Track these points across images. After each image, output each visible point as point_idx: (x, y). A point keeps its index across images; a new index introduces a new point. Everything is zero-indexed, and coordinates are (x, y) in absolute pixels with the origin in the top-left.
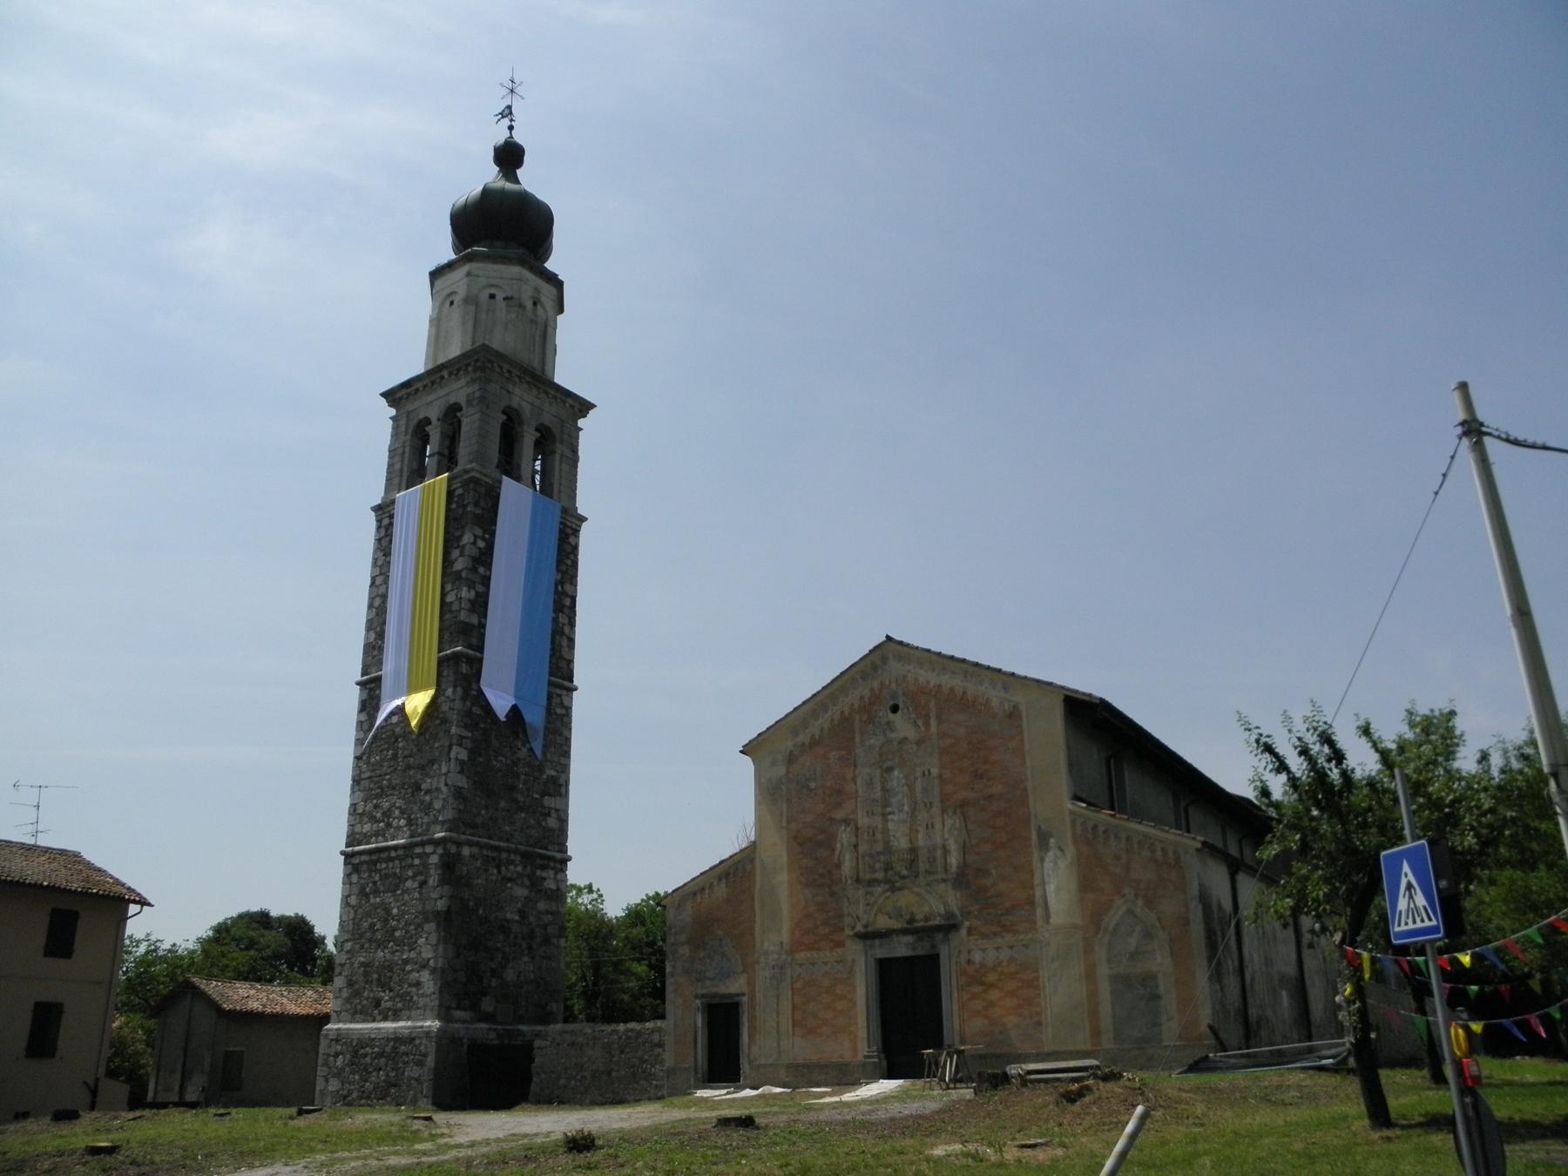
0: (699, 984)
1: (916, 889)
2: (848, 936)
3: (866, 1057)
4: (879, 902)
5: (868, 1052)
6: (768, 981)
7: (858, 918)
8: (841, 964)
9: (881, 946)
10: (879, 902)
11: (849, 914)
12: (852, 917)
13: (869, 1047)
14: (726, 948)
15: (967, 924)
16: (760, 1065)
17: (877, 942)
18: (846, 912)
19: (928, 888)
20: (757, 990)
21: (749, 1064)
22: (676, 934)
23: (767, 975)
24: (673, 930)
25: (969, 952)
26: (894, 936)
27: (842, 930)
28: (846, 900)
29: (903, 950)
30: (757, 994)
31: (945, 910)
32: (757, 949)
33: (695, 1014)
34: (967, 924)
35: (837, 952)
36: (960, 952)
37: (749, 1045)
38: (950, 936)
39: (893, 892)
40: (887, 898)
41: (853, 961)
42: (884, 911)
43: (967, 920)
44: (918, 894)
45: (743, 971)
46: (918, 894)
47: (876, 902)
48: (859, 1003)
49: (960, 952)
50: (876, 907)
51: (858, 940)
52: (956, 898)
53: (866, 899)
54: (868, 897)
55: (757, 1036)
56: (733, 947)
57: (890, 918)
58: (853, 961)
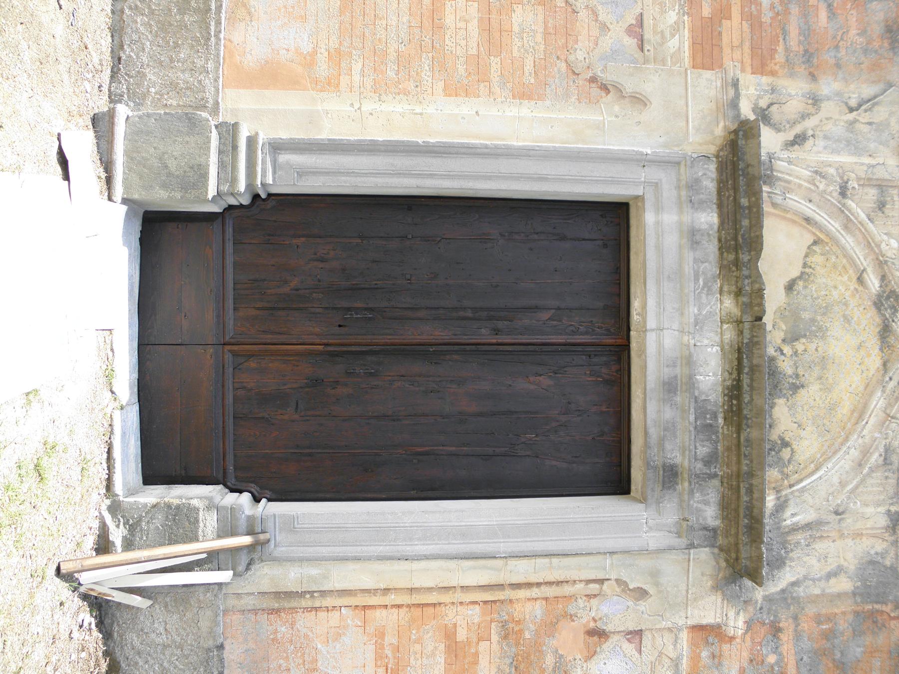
1: (878, 402)
2: (735, 84)
3: (229, 132)
4: (848, 241)
5: (251, 142)
7: (799, 140)
8: (631, 42)
9: (693, 236)
10: (848, 241)
11: (815, 101)
12: (804, 116)
13: (276, 147)
15: (736, 623)
17: (709, 219)
18: (828, 86)
19: (875, 458)
25: (635, 635)
26: (729, 303)
27: (761, 67)
28: (868, 91)
29: (669, 340)
31: (795, 529)
34: (736, 623)
35: (676, 29)
36: (641, 594)
38: (704, 555)
39: (878, 304)
40: (860, 280)
41: (639, 101)
42: (817, 259)
43: (749, 625)
44: (860, 412)
46: (860, 412)
47: (848, 225)
48: (465, 108)
49: (641, 594)
50: (834, 226)
51: (719, 131)
52: (830, 576)
53: (867, 182)
54: (872, 194)
57: (790, 287)
58: (639, 101)
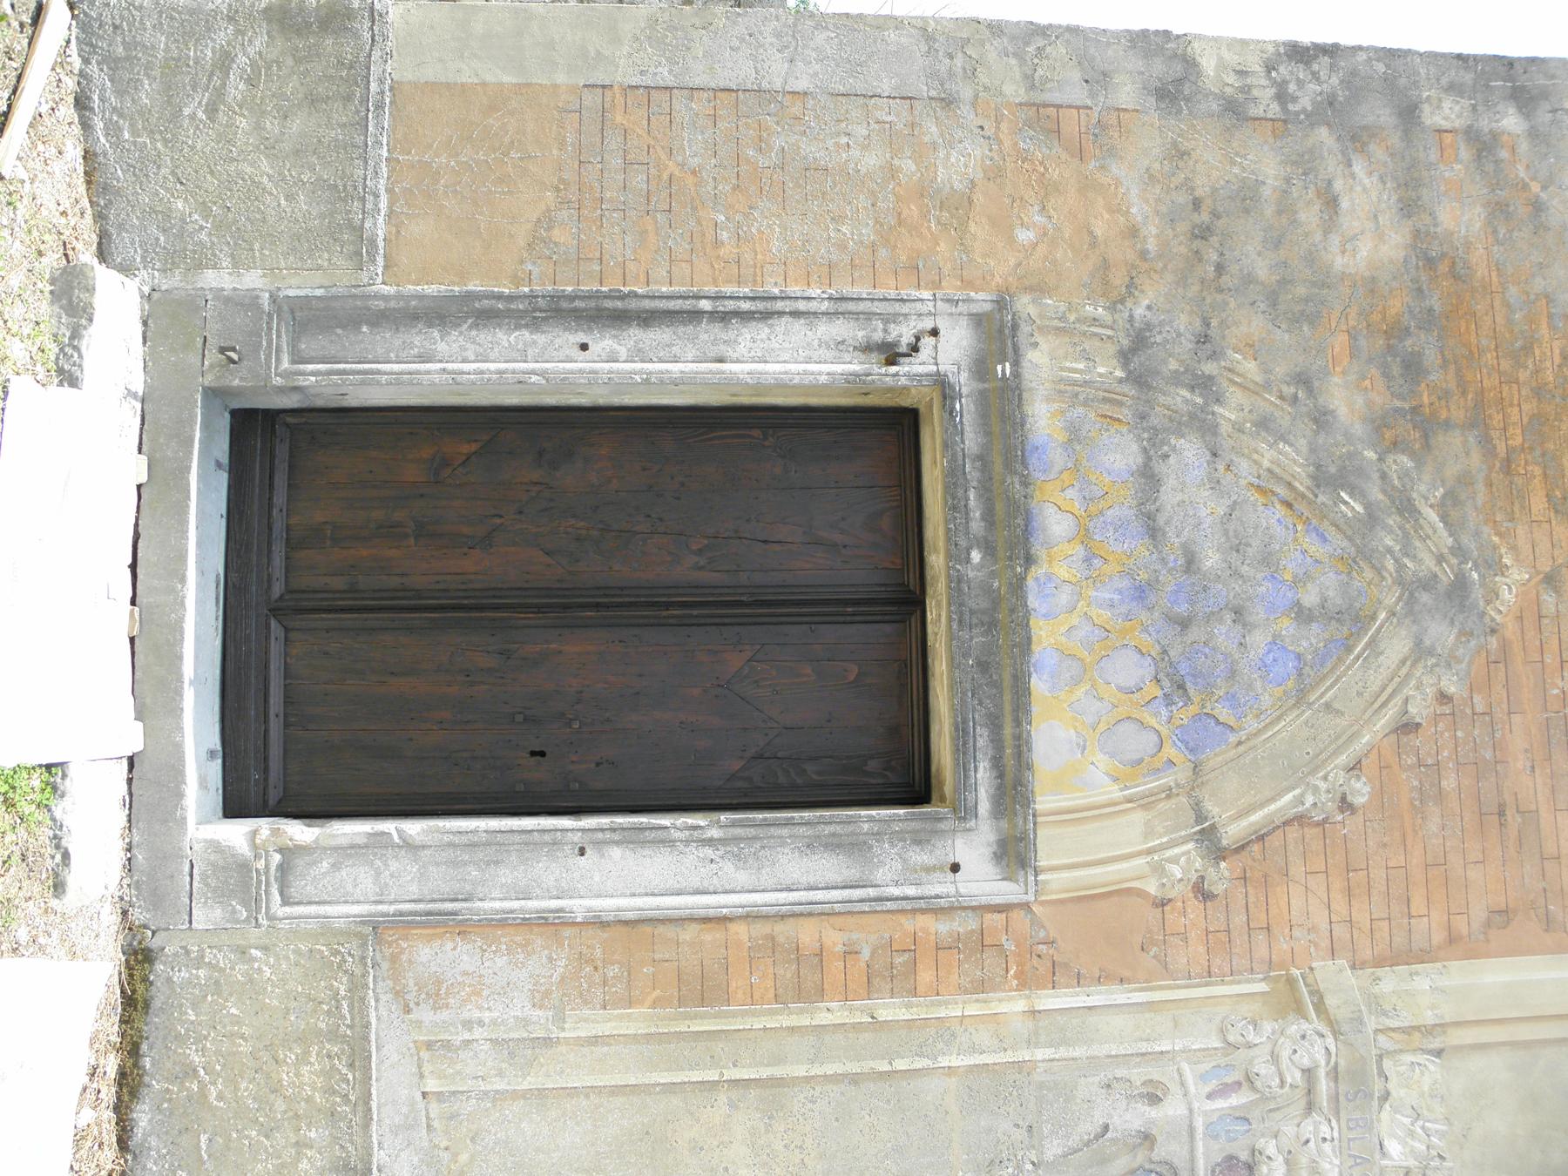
0: (1107, 369)
6: (1130, 1118)
14: (1396, 647)
16: (359, 1057)
20: (1049, 1000)
21: (377, 928)
22: (1484, 146)
23: (1173, 1108)
24: (1511, 121)
30: (1012, 1005)
32: (1390, 981)
33: (841, 307)
37: (551, 924)
45: (1208, 837)
55: (634, 1021)
56: (1406, 728)
